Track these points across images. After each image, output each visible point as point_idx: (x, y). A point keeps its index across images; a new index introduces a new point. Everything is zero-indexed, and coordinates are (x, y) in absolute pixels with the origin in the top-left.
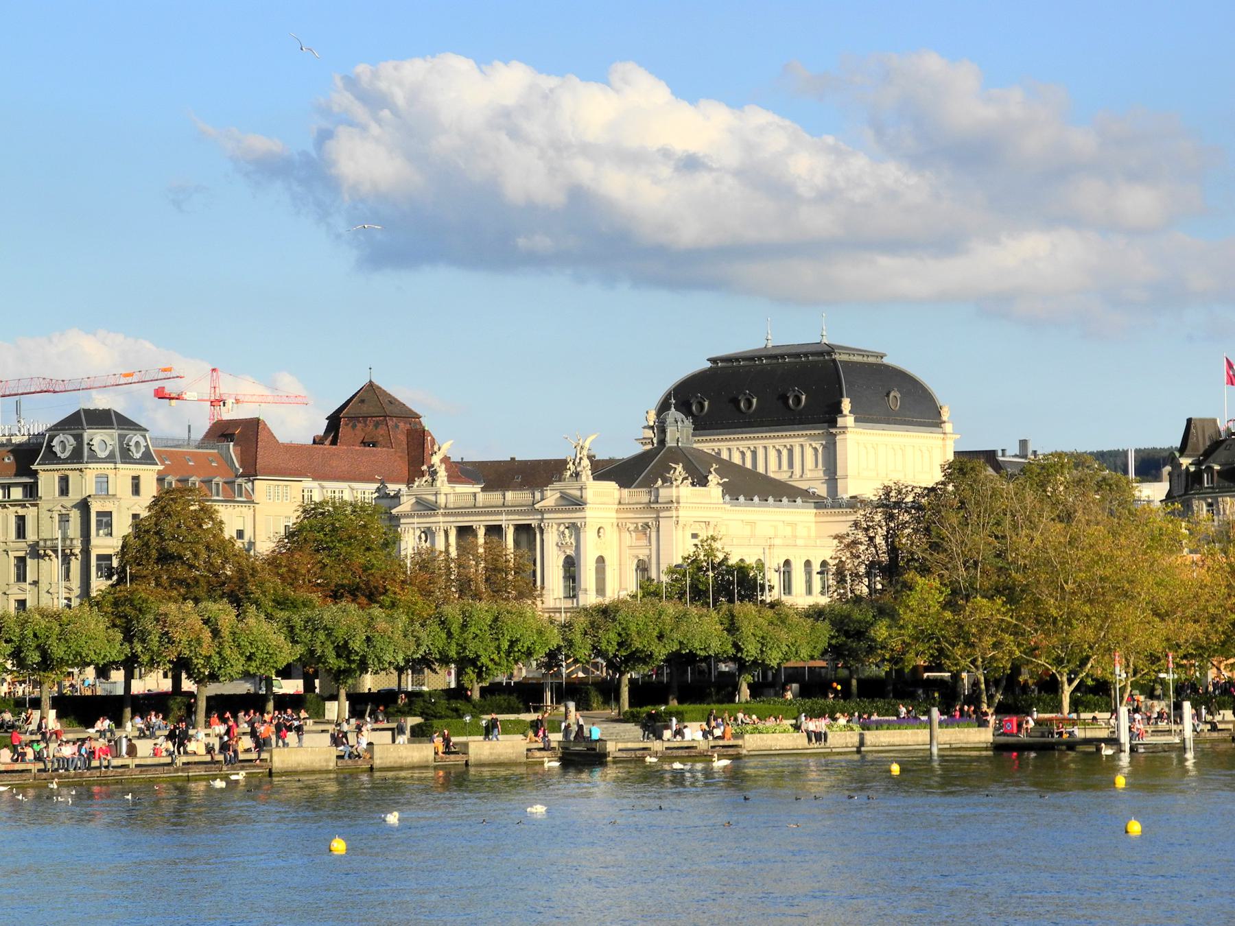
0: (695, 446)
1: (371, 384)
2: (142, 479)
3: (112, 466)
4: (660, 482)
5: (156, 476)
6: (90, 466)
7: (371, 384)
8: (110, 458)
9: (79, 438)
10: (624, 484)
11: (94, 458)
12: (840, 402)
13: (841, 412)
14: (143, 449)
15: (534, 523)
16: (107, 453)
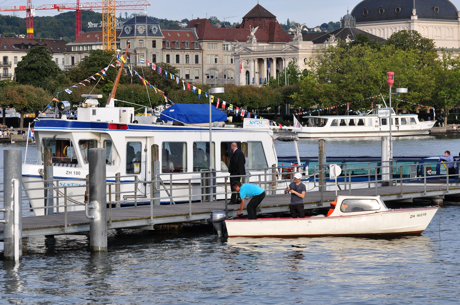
0: (357, 28)
1: (258, 5)
2: (156, 42)
3: (144, 37)
4: (326, 41)
5: (162, 41)
6: (137, 37)
7: (258, 5)
8: (144, 34)
9: (133, 27)
10: (315, 42)
11: (138, 34)
12: (412, 11)
13: (412, 14)
14: (157, 31)
15: (282, 57)
16: (143, 32)
